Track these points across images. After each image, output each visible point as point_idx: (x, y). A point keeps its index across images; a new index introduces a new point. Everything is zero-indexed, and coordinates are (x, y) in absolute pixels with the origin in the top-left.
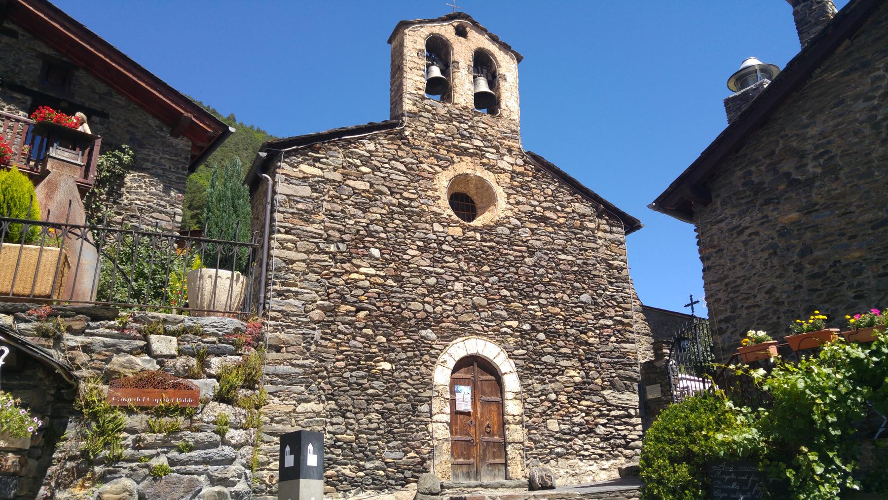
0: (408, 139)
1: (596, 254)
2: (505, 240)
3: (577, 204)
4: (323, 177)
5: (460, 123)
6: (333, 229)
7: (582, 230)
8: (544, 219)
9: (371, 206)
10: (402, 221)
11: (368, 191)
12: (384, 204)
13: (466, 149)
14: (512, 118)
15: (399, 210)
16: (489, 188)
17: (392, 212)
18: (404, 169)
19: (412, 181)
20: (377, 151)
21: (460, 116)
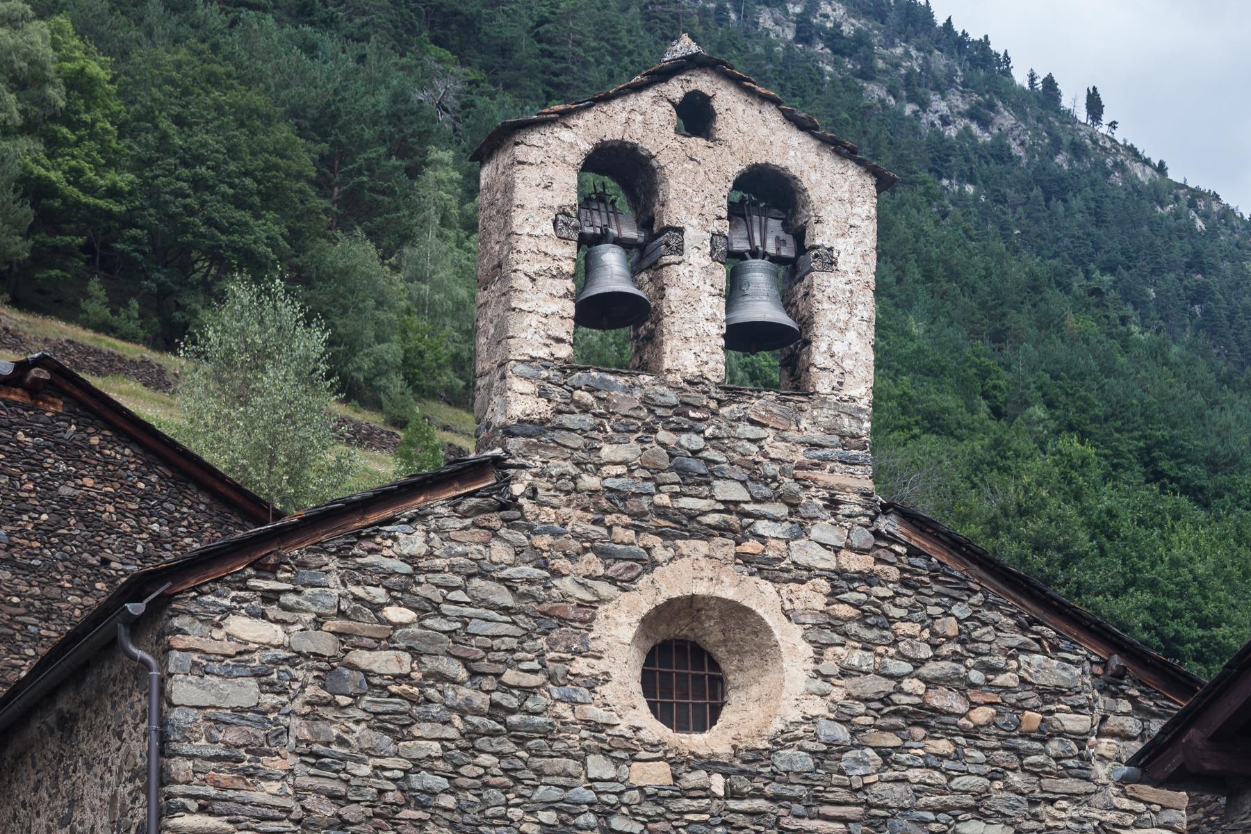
0: (520, 507)
1: (1083, 811)
2: (798, 790)
3: (1038, 658)
4: (287, 648)
5: (679, 430)
6: (317, 792)
7: (1044, 741)
8: (923, 716)
9: (415, 720)
10: (500, 755)
11: (406, 678)
12: (451, 709)
13: (692, 516)
14: (846, 392)
15: (492, 725)
16: (760, 628)
17: (472, 734)
18: (507, 600)
19: (529, 635)
20: (430, 554)
21: (682, 408)
